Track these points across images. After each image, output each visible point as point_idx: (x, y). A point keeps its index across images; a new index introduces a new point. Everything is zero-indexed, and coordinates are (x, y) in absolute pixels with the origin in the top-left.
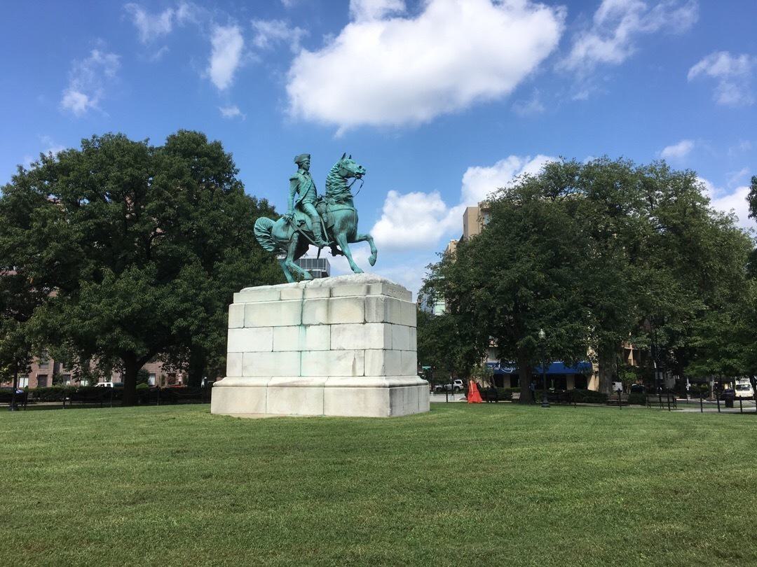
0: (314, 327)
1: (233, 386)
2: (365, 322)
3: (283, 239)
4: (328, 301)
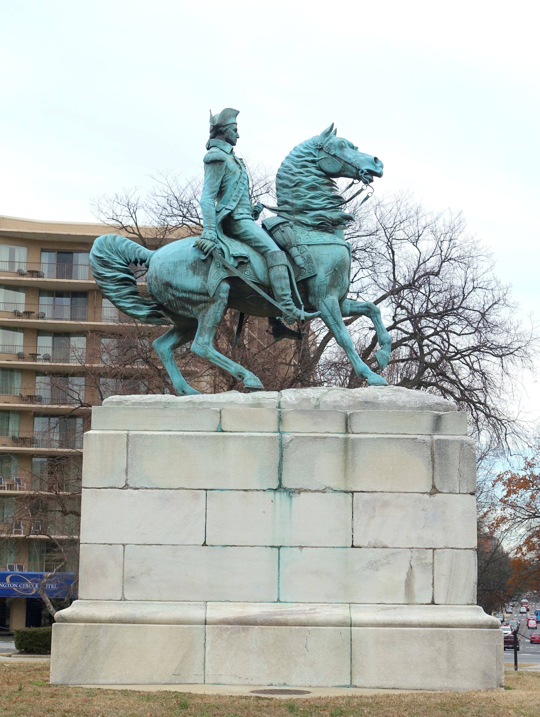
0: (310, 494)
1: (111, 621)
2: (434, 491)
3: (192, 292)
4: (346, 440)
